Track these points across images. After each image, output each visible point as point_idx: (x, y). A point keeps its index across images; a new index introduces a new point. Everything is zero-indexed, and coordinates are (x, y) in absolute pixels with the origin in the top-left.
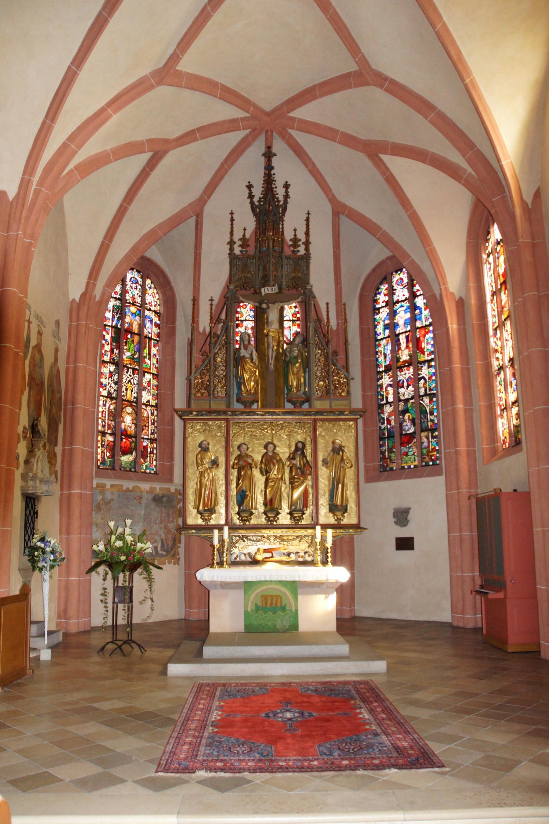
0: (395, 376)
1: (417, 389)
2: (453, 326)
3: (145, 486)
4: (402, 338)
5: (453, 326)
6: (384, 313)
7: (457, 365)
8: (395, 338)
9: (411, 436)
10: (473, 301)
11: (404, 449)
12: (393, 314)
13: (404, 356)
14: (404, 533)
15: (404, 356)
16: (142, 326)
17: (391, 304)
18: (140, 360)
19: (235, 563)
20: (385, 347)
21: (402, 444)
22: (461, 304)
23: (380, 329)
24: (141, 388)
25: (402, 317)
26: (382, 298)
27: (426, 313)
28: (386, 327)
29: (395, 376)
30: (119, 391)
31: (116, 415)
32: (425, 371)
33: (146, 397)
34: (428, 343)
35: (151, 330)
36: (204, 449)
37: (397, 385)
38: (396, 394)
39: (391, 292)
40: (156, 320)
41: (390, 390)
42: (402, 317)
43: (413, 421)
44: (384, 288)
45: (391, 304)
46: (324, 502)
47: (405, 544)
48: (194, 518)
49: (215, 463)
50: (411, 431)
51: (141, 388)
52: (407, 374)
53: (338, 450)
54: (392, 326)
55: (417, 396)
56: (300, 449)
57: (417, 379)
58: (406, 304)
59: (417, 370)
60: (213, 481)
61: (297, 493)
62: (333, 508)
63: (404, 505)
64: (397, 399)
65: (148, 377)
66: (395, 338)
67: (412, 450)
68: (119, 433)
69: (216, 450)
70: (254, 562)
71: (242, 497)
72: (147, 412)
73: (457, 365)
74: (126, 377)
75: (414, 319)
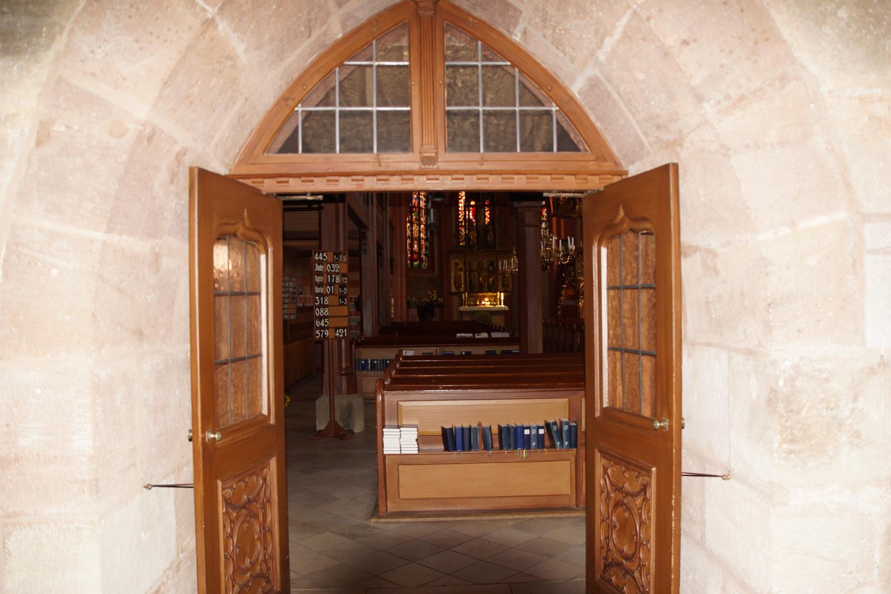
3: (424, 275)
16: (419, 203)
18: (419, 220)
19: (469, 305)
24: (420, 232)
30: (412, 234)
31: (412, 245)
33: (422, 235)
35: (422, 204)
36: (457, 264)
40: (424, 199)
46: (500, 283)
48: (453, 290)
49: (461, 270)
51: (420, 232)
56: (492, 264)
60: (460, 276)
61: (491, 280)
62: (503, 285)
65: (422, 226)
68: (412, 252)
69: (461, 266)
70: (476, 305)
71: (471, 282)
72: (423, 242)
74: (414, 228)
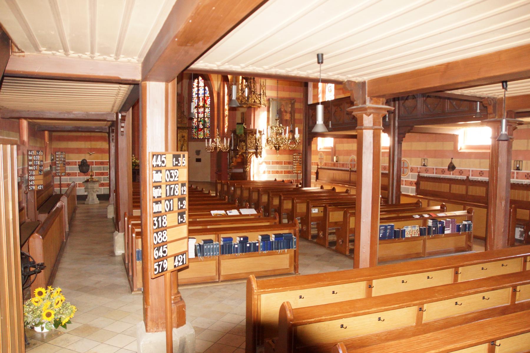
0: (198, 110)
1: (204, 115)
2: (216, 100)
4: (201, 99)
5: (216, 100)
6: (195, 90)
7: (216, 112)
8: (198, 98)
9: (202, 129)
10: (222, 94)
11: (199, 133)
12: (198, 90)
13: (201, 104)
14: (198, 157)
15: (201, 104)
17: (198, 87)
20: (195, 100)
21: (199, 131)
22: (218, 94)
23: (194, 94)
25: (201, 92)
26: (195, 84)
27: (208, 92)
28: (196, 94)
29: (198, 110)
32: (207, 110)
34: (208, 102)
37: (198, 113)
38: (198, 115)
39: (198, 83)
41: (196, 114)
42: (201, 92)
43: (203, 125)
44: (196, 81)
45: (198, 87)
47: (198, 160)
50: (202, 127)
52: (201, 110)
53: (183, 137)
54: (198, 94)
55: (204, 117)
57: (204, 112)
58: (203, 88)
59: (204, 109)
63: (198, 149)
64: (198, 117)
66: (198, 98)
67: (202, 133)
73: (216, 112)
75: (205, 93)
